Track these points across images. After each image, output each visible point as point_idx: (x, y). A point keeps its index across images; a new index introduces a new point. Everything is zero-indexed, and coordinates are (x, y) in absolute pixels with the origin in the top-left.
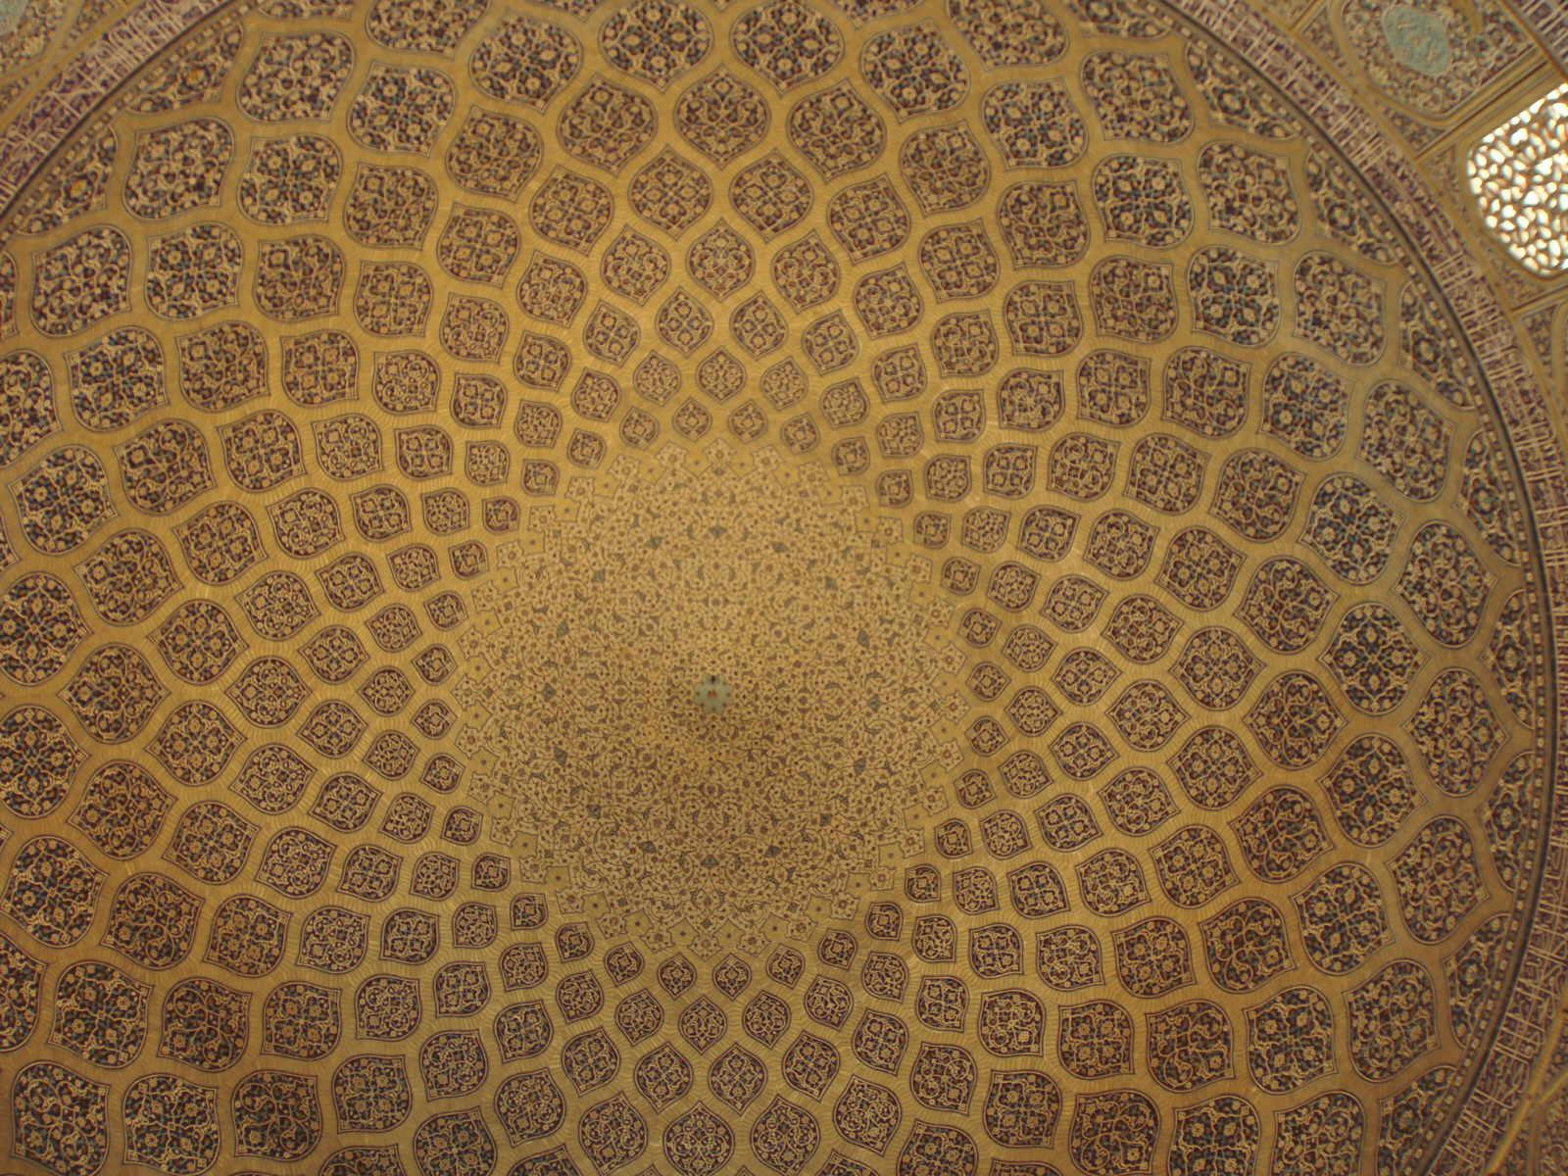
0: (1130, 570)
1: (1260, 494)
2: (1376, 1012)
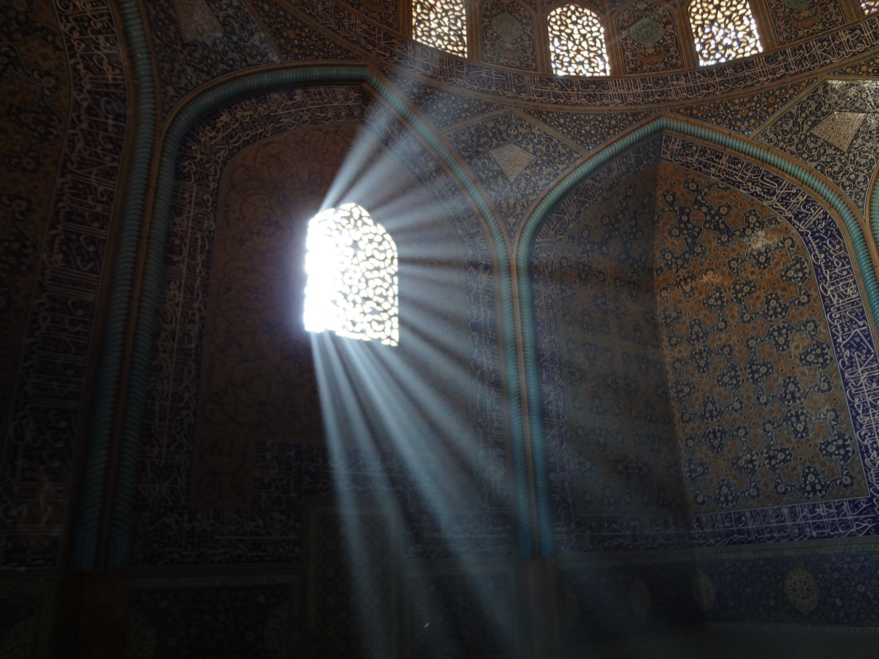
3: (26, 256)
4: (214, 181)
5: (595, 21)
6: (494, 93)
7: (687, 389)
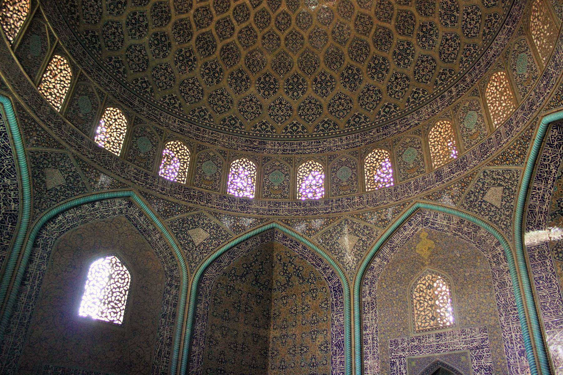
0: (235, 12)
1: (230, 56)
2: (116, 31)
5: (254, 168)
7: (276, 353)
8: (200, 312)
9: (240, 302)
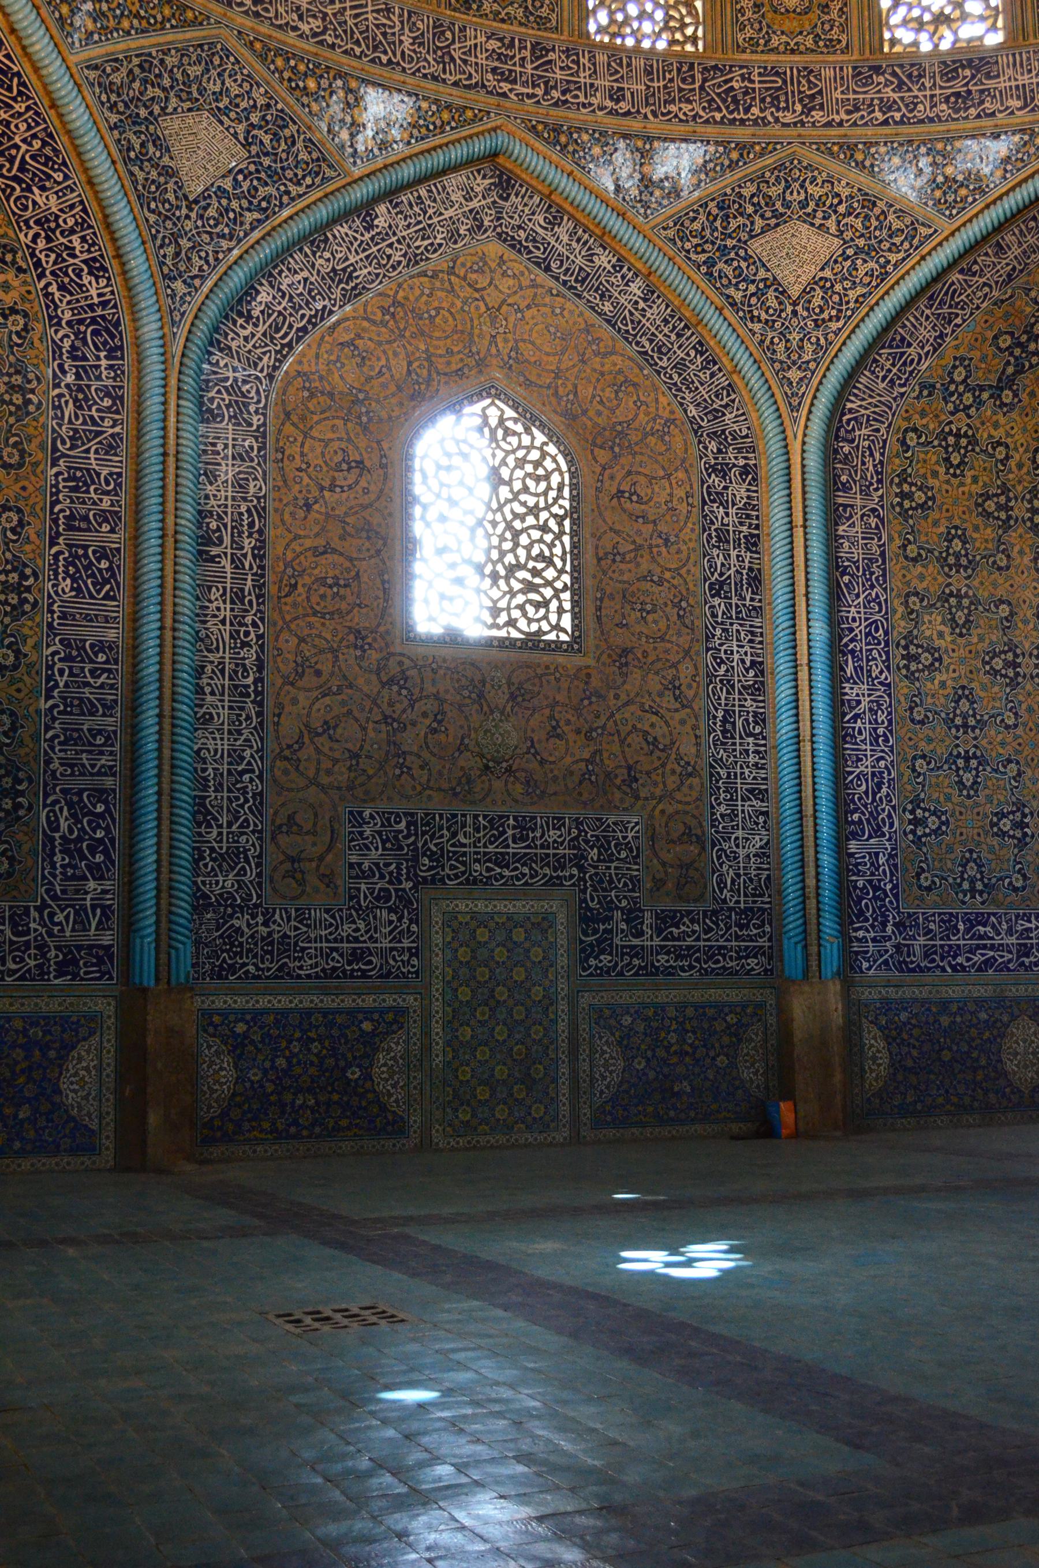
3: (28, 589)
4: (257, 412)
6: (755, 122)
8: (852, 552)
9: (1005, 489)
